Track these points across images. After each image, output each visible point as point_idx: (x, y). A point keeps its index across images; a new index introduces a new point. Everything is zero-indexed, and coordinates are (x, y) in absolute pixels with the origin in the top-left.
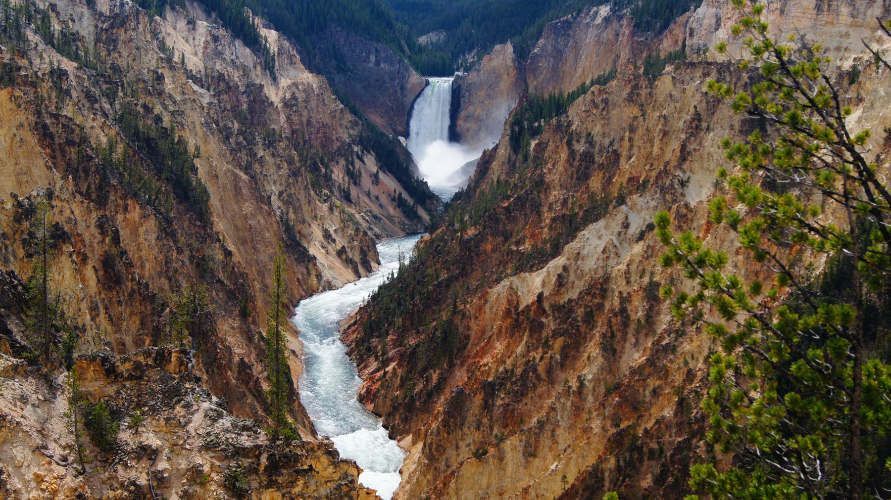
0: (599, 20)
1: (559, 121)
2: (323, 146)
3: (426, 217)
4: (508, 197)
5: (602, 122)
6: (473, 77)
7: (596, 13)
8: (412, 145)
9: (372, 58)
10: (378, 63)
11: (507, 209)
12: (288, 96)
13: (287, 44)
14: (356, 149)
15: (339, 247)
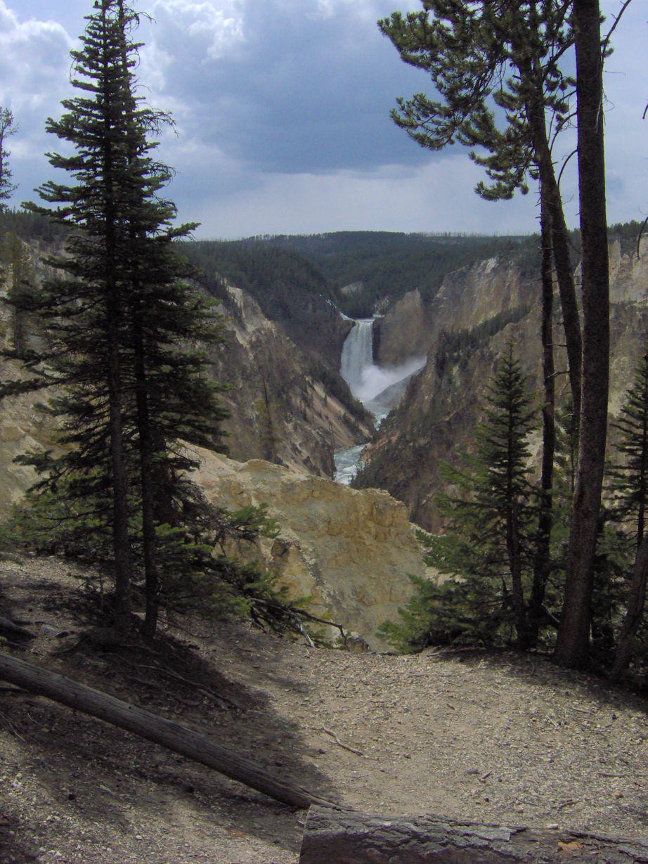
0: (488, 271)
1: (482, 352)
2: (283, 378)
3: (366, 432)
4: (448, 414)
5: (520, 352)
6: (389, 318)
7: (485, 265)
8: (346, 374)
9: (310, 306)
10: (314, 310)
11: (449, 423)
12: (254, 339)
13: (250, 298)
14: (307, 379)
15: (305, 457)
